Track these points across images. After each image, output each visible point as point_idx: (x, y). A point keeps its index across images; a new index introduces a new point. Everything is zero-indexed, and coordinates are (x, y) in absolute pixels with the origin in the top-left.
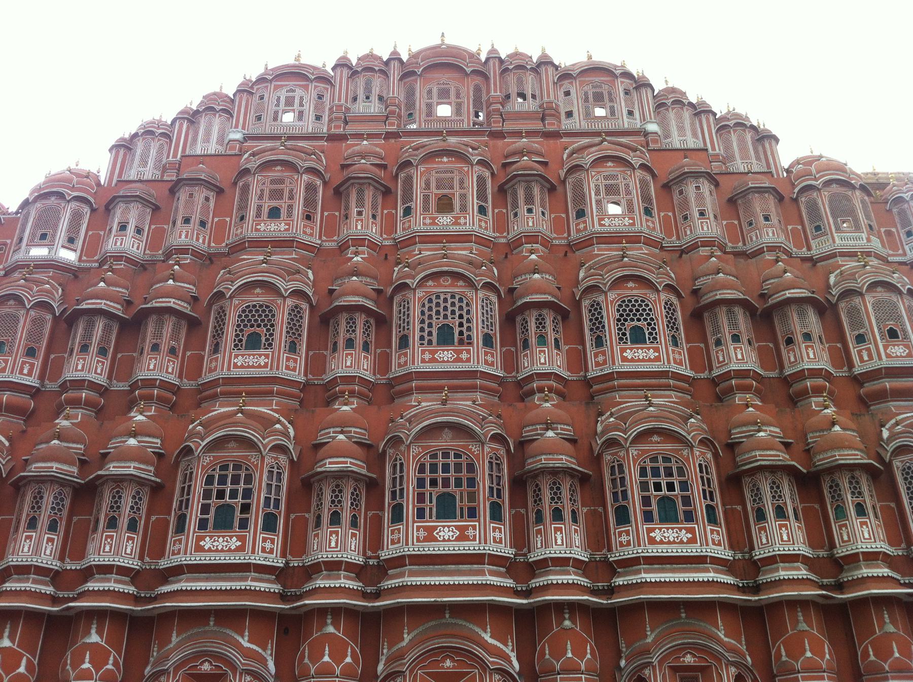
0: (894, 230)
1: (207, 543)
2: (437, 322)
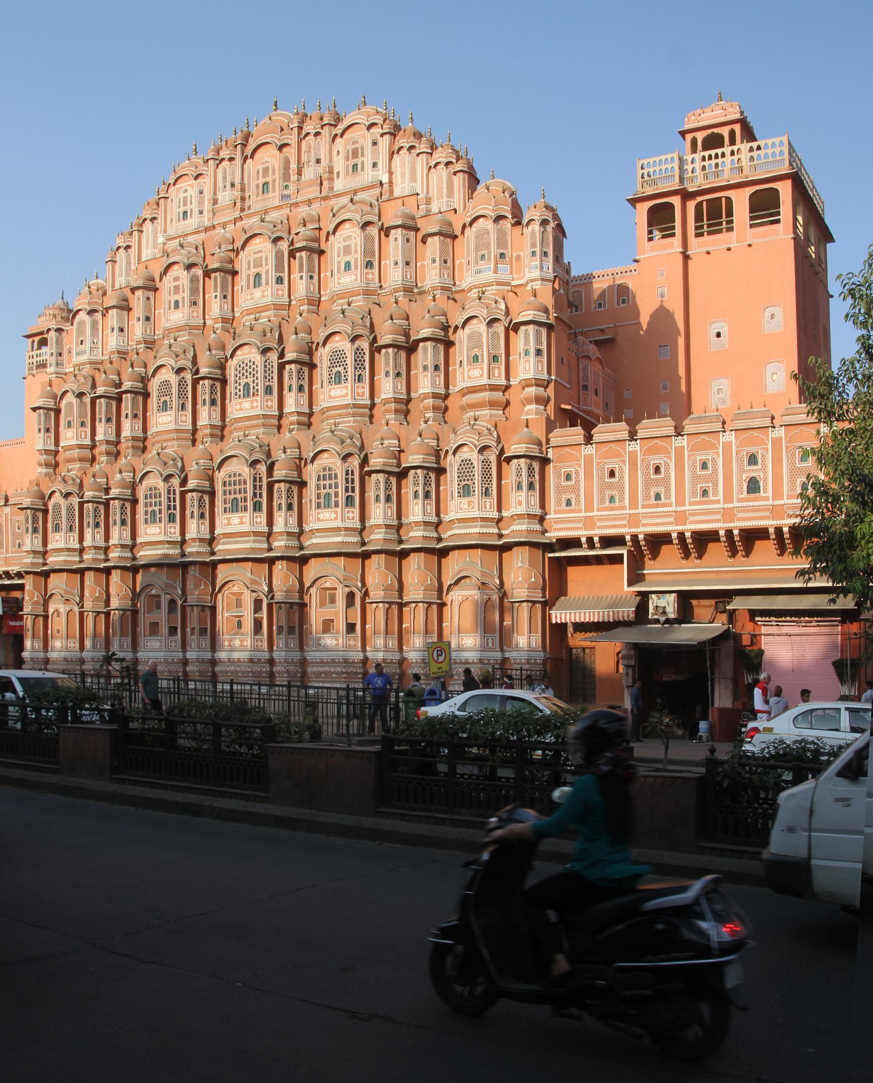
0: (522, 254)
1: (148, 531)
2: (243, 381)
